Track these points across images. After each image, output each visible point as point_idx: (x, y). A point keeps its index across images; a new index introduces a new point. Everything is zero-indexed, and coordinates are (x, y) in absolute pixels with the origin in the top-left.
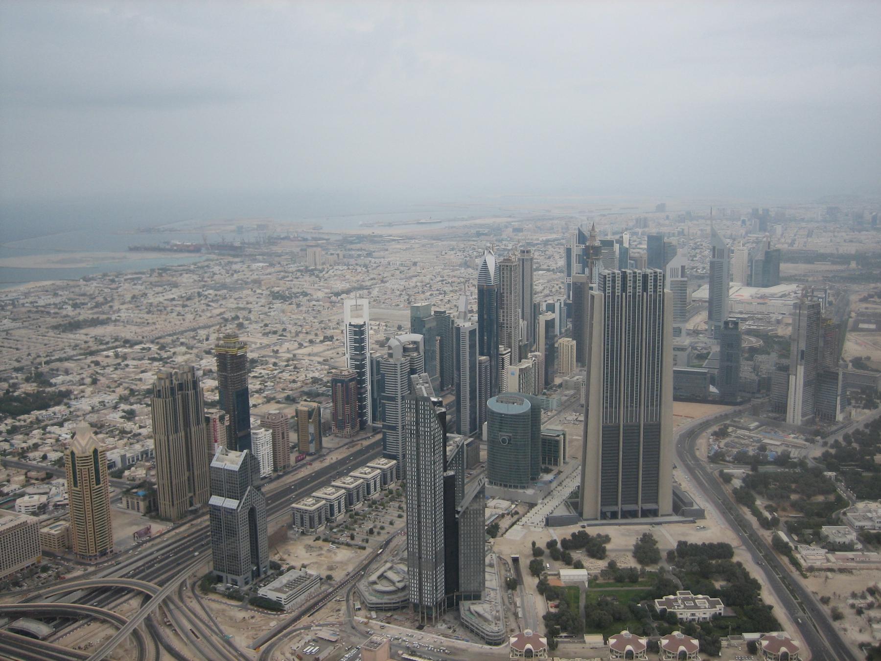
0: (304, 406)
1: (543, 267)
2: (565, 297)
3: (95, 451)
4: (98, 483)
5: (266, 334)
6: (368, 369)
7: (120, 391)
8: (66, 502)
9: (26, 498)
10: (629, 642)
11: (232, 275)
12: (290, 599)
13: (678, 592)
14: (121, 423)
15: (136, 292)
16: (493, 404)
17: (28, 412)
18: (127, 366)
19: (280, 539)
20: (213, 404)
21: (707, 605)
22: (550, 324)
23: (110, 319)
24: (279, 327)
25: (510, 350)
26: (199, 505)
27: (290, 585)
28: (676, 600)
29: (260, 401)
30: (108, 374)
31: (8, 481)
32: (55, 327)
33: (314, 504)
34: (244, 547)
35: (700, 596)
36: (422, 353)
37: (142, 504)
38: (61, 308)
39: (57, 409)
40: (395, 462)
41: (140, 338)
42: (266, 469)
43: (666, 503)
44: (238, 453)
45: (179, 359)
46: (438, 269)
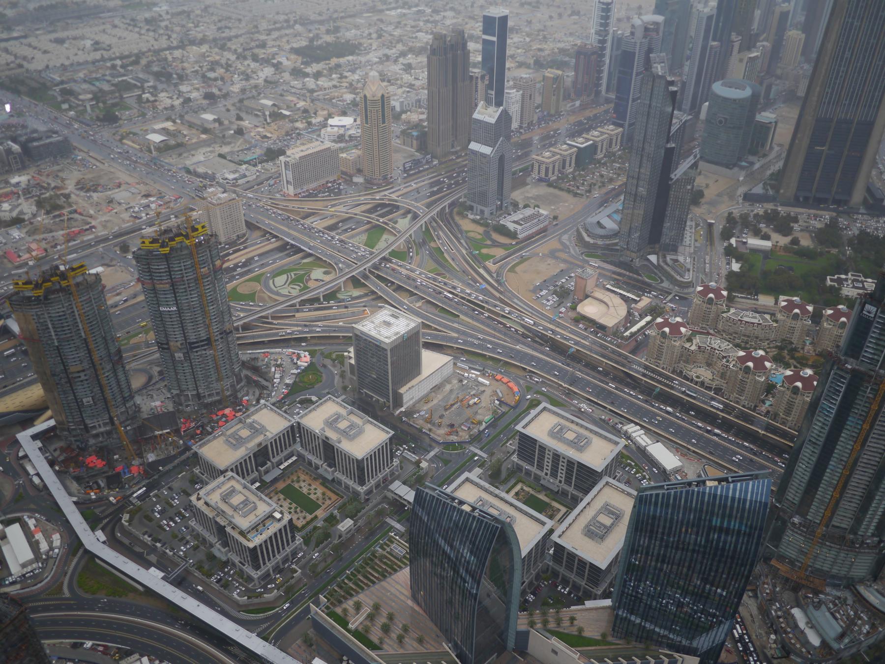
0: (550, 73)
3: (383, 96)
4: (384, 122)
6: (609, 45)
7: (400, 47)
8: (358, 135)
9: (329, 129)
10: (797, 306)
12: (523, 231)
16: (718, 88)
17: (329, 59)
18: (406, 25)
19: (520, 183)
20: (475, 65)
22: (784, 15)
25: (740, 38)
26: (458, 148)
27: (526, 219)
28: (846, 280)
29: (513, 65)
31: (315, 114)
33: (550, 158)
34: (493, 185)
35: (870, 280)
36: (661, 34)
37: (415, 142)
39: (350, 58)
40: (621, 129)
42: (515, 125)
43: (858, 196)
44: (496, 109)
45: (448, 22)
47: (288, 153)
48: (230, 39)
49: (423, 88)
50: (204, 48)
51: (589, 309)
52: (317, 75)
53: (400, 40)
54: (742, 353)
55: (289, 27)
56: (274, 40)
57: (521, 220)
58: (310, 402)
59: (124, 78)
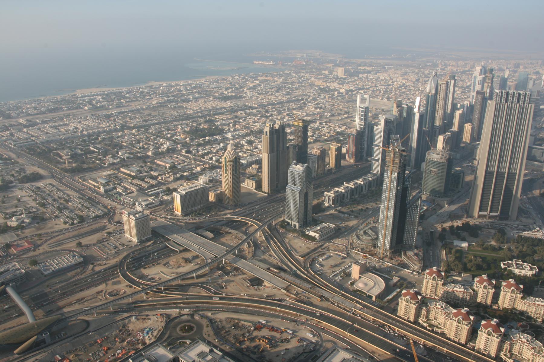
1: (460, 85)
2: (471, 101)
3: (236, 158)
5: (316, 108)
7: (245, 131)
8: (221, 180)
11: (301, 78)
12: (321, 236)
13: (514, 260)
14: (246, 146)
15: (255, 84)
18: (250, 119)
21: (529, 268)
23: (243, 96)
24: (323, 106)
30: (241, 122)
31: (196, 168)
32: (219, 98)
35: (525, 264)
37: (254, 184)
38: (221, 89)
41: (256, 106)
46: (404, 81)
47: (179, 190)
48: (149, 126)
49: (260, 154)
50: (134, 131)
51: (360, 286)
52: (199, 145)
53: (246, 127)
54: (454, 311)
55: (183, 120)
56: (174, 126)
57: (318, 230)
58: (186, 343)
59: (89, 147)
